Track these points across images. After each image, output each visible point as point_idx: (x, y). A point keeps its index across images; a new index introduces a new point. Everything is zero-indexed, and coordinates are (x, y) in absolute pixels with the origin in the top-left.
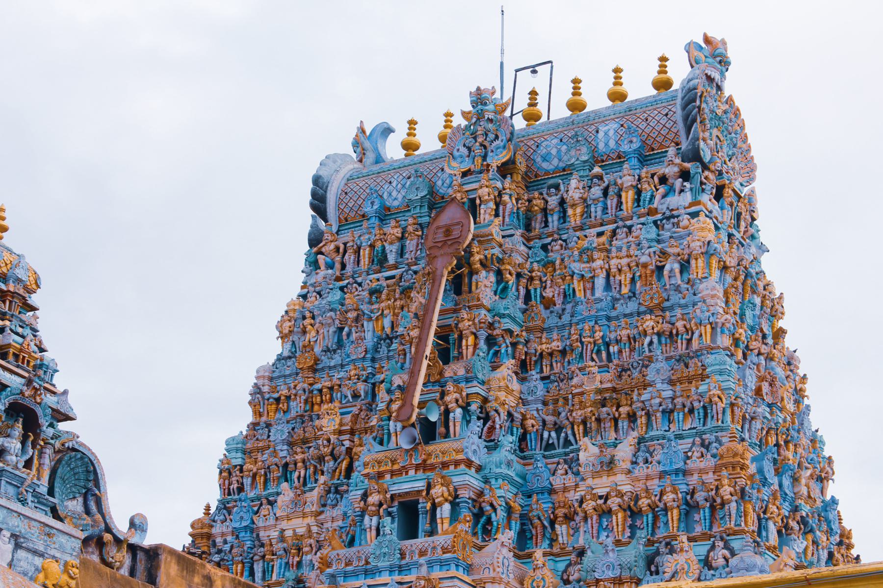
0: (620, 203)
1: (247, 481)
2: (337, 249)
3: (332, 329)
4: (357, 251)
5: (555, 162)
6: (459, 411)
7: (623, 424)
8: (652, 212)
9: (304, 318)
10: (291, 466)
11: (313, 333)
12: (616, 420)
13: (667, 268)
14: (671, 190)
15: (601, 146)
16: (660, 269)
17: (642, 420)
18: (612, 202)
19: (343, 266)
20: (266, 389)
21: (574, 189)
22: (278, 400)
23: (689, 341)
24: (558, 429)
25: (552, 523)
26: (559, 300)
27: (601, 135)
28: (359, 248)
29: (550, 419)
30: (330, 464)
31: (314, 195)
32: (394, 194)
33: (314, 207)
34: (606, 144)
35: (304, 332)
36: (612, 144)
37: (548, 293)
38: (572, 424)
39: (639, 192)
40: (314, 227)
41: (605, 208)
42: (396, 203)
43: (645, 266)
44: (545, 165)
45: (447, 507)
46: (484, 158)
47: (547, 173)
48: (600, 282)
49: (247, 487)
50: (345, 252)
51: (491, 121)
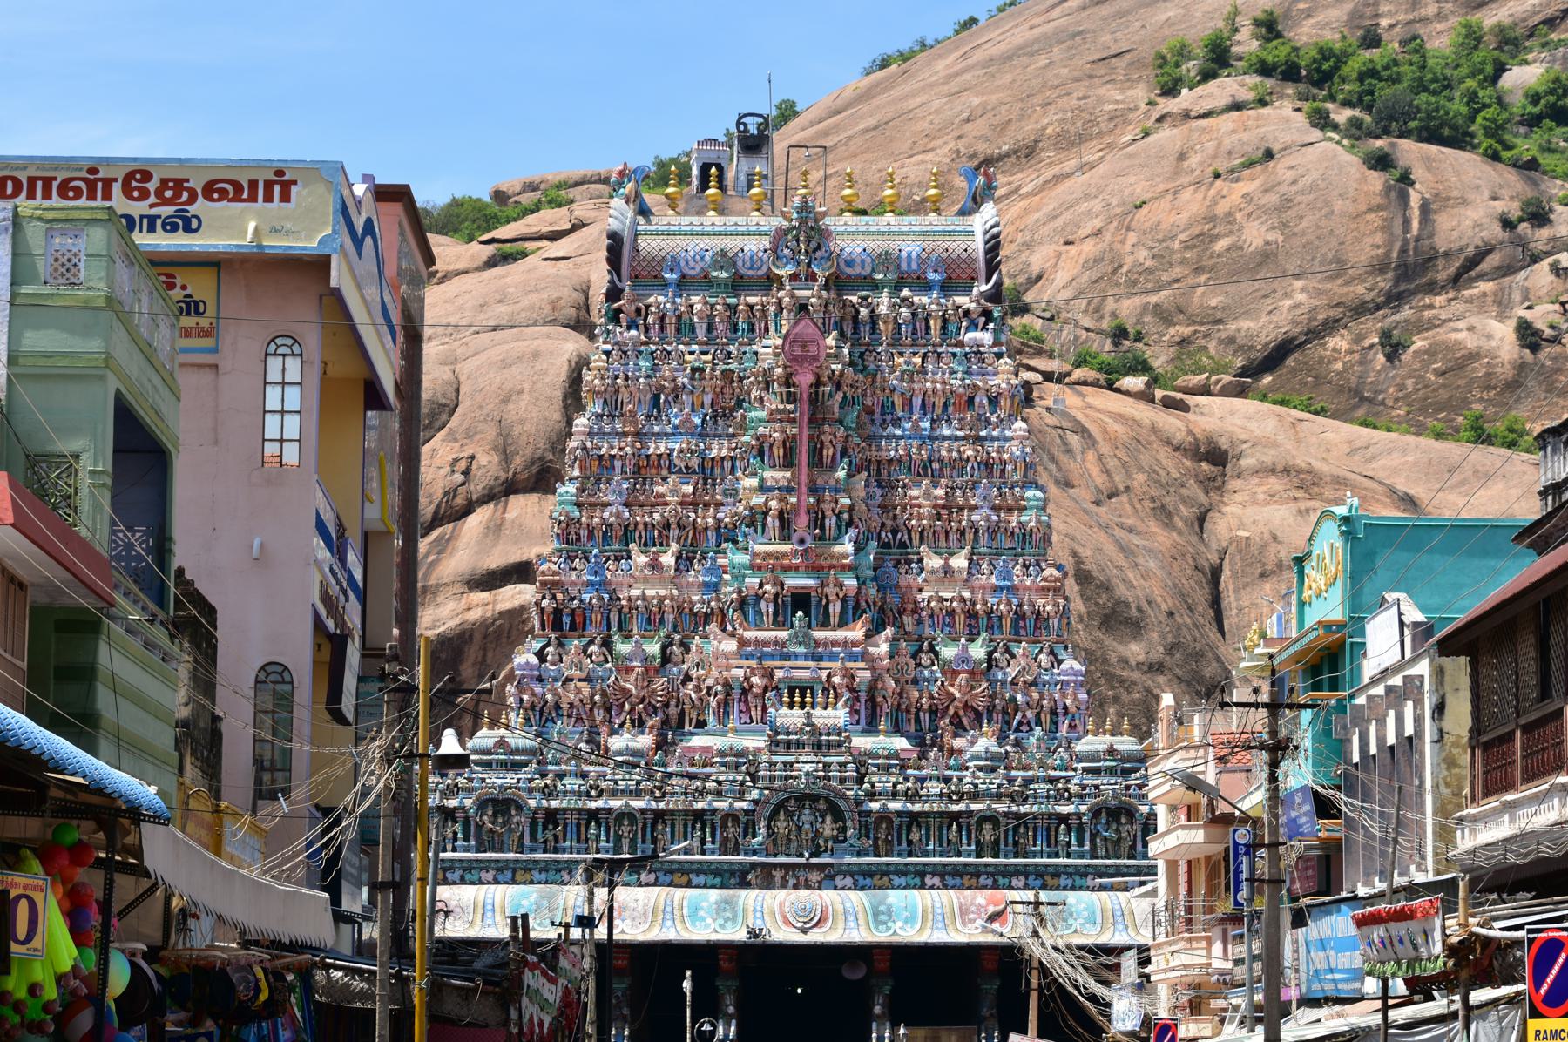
0: (928, 328)
1: (584, 533)
2: (638, 311)
3: (649, 396)
4: (662, 319)
5: (857, 270)
6: (834, 519)
7: (953, 537)
8: (961, 344)
9: (617, 377)
10: (631, 527)
11: (626, 395)
12: (947, 533)
13: (977, 400)
14: (973, 326)
15: (904, 266)
16: (971, 400)
17: (969, 536)
18: (920, 325)
19: (647, 330)
20: (589, 444)
21: (883, 303)
22: (601, 457)
23: (1003, 471)
24: (895, 532)
25: (901, 614)
26: (878, 410)
27: (904, 254)
28: (664, 315)
29: (889, 523)
30: (674, 532)
31: (610, 249)
32: (692, 264)
33: (609, 260)
34: (909, 265)
35: (617, 391)
36: (914, 266)
37: (868, 402)
38: (910, 532)
39: (945, 321)
40: (611, 282)
41: (915, 328)
42: (692, 273)
43: (960, 396)
44: (849, 271)
45: (838, 604)
46: (809, 265)
47: (849, 276)
48: (917, 402)
49: (584, 540)
50: (647, 315)
51: (812, 228)
